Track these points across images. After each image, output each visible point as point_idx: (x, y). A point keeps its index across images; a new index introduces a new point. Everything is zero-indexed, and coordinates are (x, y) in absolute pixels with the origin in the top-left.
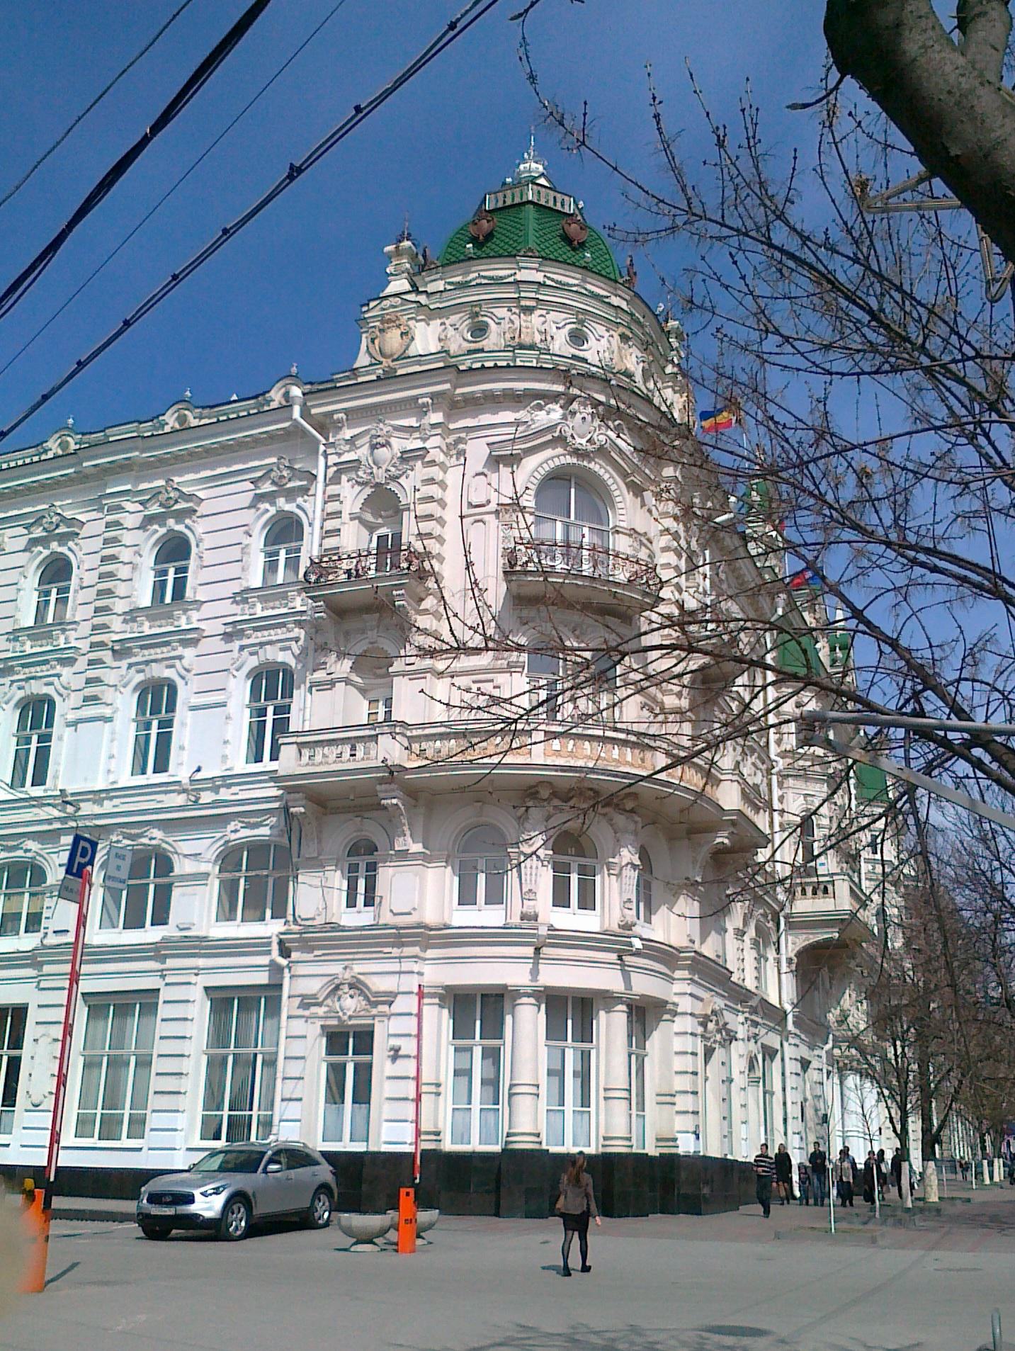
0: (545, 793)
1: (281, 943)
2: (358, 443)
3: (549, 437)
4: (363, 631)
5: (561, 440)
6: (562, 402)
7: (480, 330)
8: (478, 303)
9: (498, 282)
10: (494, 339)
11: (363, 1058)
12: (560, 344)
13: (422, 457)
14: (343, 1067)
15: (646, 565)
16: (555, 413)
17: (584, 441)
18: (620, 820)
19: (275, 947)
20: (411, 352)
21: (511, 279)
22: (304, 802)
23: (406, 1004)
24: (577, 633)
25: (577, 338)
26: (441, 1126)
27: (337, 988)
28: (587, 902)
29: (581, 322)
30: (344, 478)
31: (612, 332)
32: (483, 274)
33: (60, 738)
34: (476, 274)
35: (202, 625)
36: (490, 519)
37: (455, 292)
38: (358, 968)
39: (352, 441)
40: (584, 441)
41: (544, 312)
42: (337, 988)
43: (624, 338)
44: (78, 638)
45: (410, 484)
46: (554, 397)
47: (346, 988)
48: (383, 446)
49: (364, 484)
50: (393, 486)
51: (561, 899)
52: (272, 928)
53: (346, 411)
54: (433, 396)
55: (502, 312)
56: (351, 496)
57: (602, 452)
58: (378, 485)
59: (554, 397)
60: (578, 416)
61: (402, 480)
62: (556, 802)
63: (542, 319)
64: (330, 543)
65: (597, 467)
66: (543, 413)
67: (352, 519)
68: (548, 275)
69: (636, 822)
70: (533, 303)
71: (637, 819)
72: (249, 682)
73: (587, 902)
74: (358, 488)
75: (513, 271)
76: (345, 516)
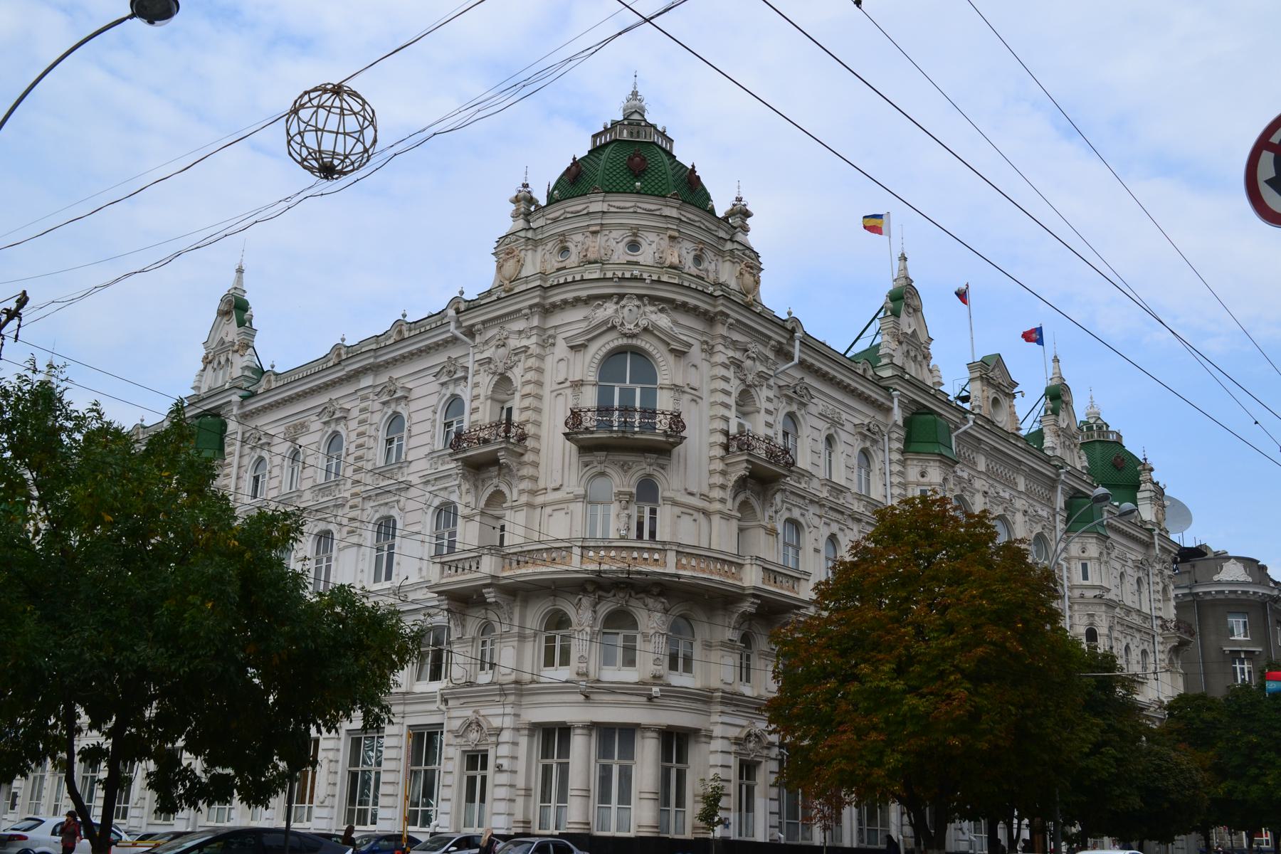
0: (590, 588)
1: (442, 695)
2: (490, 344)
3: (604, 328)
4: (491, 478)
6: (615, 300)
7: (564, 250)
8: (563, 234)
9: (577, 215)
10: (573, 259)
11: (483, 772)
12: (620, 253)
13: (526, 352)
14: (475, 778)
15: (671, 414)
17: (632, 326)
18: (650, 601)
19: (439, 698)
20: (523, 274)
22: (446, 602)
23: (506, 736)
24: (625, 468)
25: (634, 246)
26: (531, 818)
27: (469, 725)
28: (630, 662)
29: (635, 235)
30: (482, 370)
31: (661, 236)
32: (567, 210)
33: (336, 559)
34: (563, 211)
35: (410, 478)
37: (552, 225)
38: (482, 712)
40: (632, 326)
41: (607, 232)
42: (469, 725)
43: (672, 238)
44: (346, 491)
46: (606, 297)
47: (474, 726)
50: (509, 374)
52: (436, 686)
53: (484, 323)
54: (531, 307)
55: (578, 237)
56: (486, 382)
57: (646, 329)
58: (501, 374)
59: (606, 297)
60: (626, 309)
62: (601, 593)
63: (606, 238)
64: (475, 417)
65: (645, 343)
66: (602, 309)
67: (487, 399)
68: (611, 203)
69: (663, 603)
70: (598, 228)
71: (663, 600)
73: (630, 662)
74: (491, 376)
75: (584, 206)
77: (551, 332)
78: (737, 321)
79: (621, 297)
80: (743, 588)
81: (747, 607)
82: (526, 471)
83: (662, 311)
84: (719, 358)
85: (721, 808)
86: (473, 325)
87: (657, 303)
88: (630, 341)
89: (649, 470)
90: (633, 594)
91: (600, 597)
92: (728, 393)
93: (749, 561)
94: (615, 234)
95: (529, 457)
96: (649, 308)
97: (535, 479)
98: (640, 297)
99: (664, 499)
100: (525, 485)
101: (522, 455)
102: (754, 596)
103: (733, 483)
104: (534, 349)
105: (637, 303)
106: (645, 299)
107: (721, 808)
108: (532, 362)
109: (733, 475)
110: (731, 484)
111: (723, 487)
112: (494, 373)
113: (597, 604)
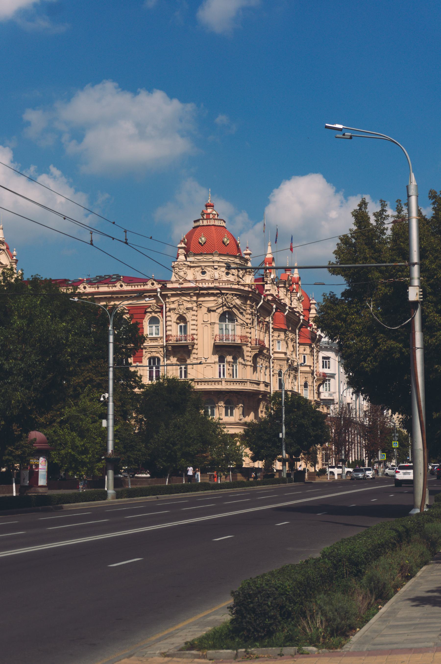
10: (207, 277)
21: (211, 260)
30: (171, 311)
36: (209, 325)
39: (173, 302)
45: (189, 316)
48: (181, 305)
49: (177, 314)
50: (184, 315)
51: (226, 414)
55: (209, 269)
58: (180, 315)
61: (187, 314)
70: (217, 267)
72: (148, 360)
73: (232, 414)
74: (175, 315)
76: (173, 321)
77: (201, 303)
79: (227, 294)
85: (40, 469)
96: (235, 298)
98: (232, 294)
99: (239, 363)
103: (253, 355)
104: (195, 308)
106: (234, 295)
107: (40, 469)
108: (194, 313)
110: (252, 356)
112: (177, 314)
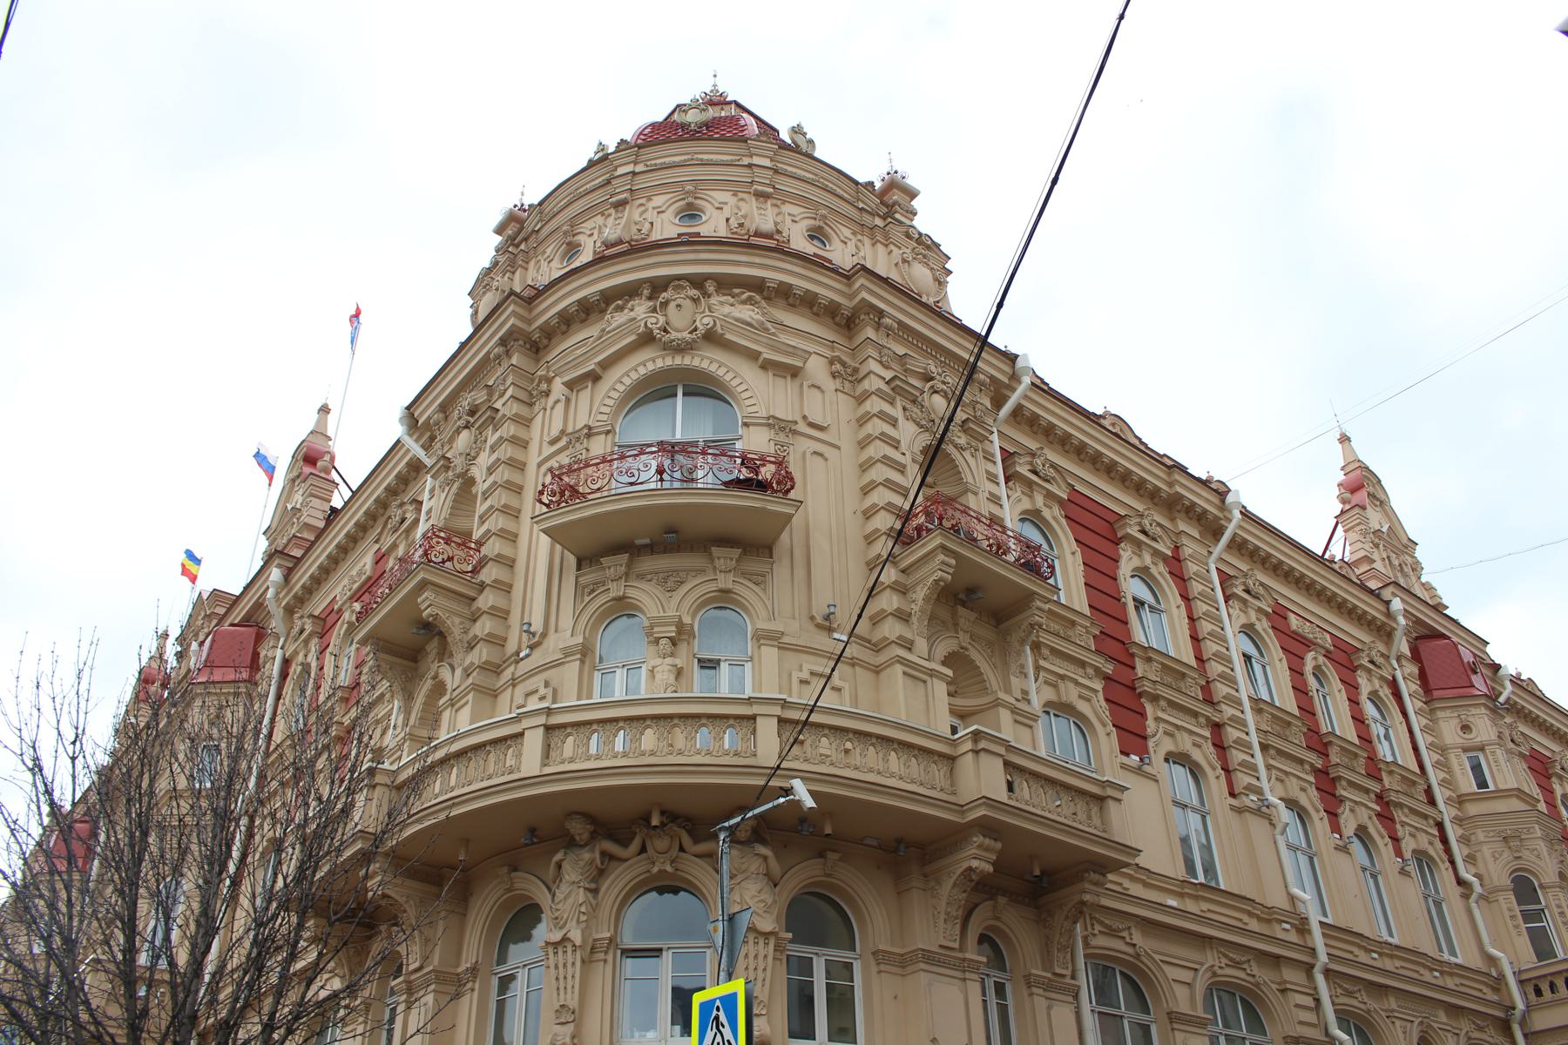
5: (647, 339)
16: (640, 309)
41: (643, 201)
54: (503, 342)
68: (648, 163)
69: (765, 858)
78: (900, 323)
80: (961, 808)
81: (976, 858)
82: (484, 626)
83: (749, 301)
84: (872, 384)
86: (429, 418)
87: (737, 291)
88: (678, 360)
89: (725, 581)
90: (687, 841)
91: (608, 857)
92: (895, 444)
93: (969, 745)
94: (658, 201)
95: (487, 600)
97: (497, 641)
100: (481, 654)
101: (474, 599)
102: (987, 827)
103: (920, 602)
105: (694, 292)
109: (918, 588)
111: (903, 616)
113: (601, 873)
